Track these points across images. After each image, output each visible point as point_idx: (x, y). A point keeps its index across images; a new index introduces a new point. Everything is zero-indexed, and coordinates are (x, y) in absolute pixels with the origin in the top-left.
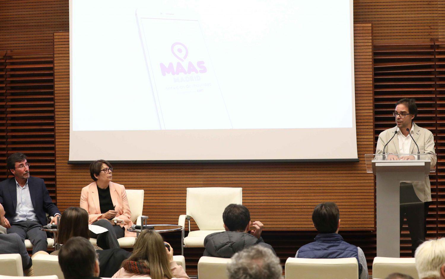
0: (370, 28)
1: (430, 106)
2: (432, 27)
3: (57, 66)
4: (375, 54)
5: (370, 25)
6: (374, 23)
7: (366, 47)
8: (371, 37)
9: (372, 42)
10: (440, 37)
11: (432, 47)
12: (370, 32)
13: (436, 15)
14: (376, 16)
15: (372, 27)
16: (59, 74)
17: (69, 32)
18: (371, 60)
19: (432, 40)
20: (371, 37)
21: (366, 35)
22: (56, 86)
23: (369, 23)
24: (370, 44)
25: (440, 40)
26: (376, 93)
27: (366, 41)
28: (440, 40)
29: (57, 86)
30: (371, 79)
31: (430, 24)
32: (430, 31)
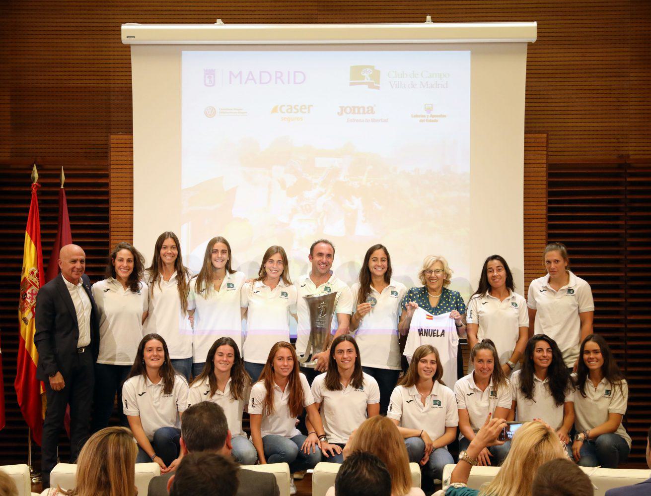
0: (545, 140)
1: (616, 244)
2: (621, 140)
3: (115, 183)
4: (550, 175)
5: (545, 135)
6: (550, 134)
7: (538, 165)
8: (545, 153)
9: (547, 159)
10: (631, 153)
11: (620, 166)
12: (545, 145)
13: (627, 124)
14: (546, 125)
15: (548, 139)
16: (118, 192)
17: (132, 135)
18: (545, 183)
19: (621, 157)
20: (545, 153)
21: (540, 149)
22: (112, 208)
23: (544, 133)
24: (544, 161)
25: (631, 157)
26: (550, 227)
27: (539, 157)
28: (631, 157)
29: (115, 209)
30: (544, 208)
31: (619, 137)
32: (618, 145)
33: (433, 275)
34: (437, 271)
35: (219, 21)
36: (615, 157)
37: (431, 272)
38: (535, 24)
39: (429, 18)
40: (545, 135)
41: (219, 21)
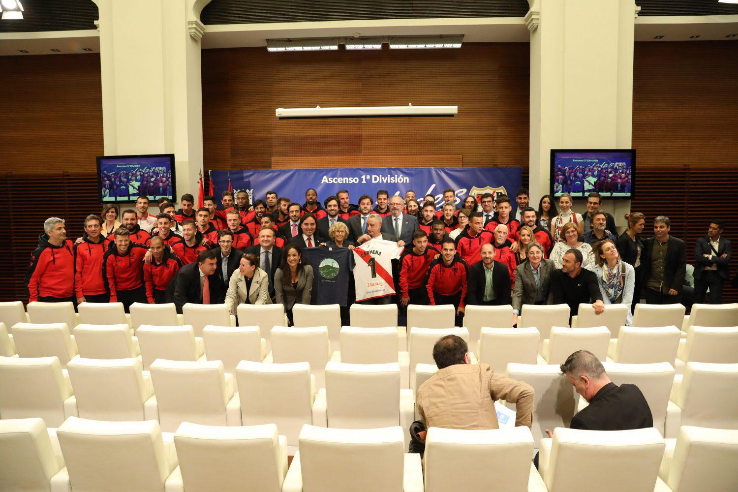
5: (462, 156)
10: (499, 164)
15: (463, 157)
19: (495, 165)
33: (341, 233)
34: (342, 231)
35: (318, 107)
36: (492, 166)
37: (339, 231)
38: (456, 107)
39: (410, 104)
40: (462, 156)
41: (318, 107)
